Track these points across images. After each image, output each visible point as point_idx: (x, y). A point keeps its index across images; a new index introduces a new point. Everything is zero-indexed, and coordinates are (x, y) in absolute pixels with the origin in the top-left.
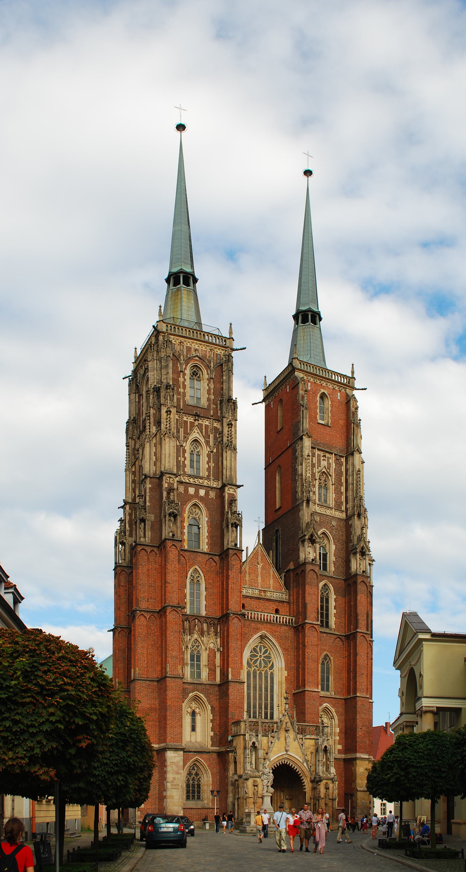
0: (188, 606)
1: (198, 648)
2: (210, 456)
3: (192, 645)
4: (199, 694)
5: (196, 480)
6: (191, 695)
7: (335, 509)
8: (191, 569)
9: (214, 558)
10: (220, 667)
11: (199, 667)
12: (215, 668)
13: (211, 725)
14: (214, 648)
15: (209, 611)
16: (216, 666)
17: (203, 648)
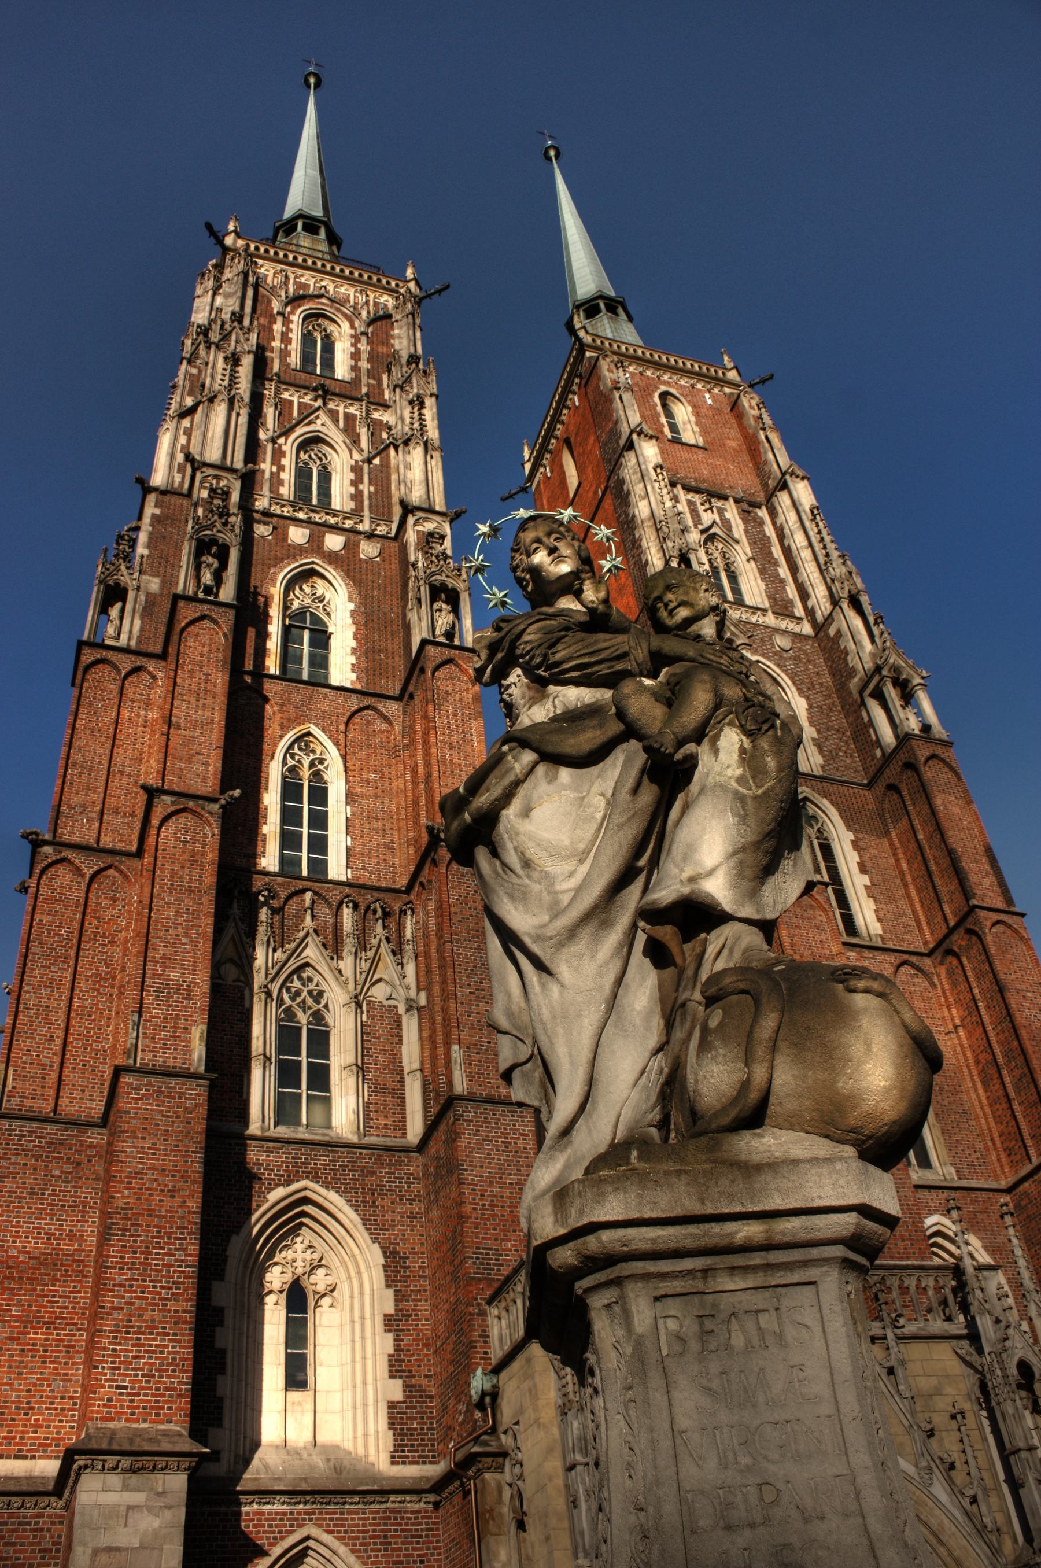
1: (318, 1002)
2: (361, 469)
4: (323, 1191)
5: (312, 515)
7: (774, 613)
8: (291, 733)
10: (421, 1070)
12: (402, 1081)
13: (386, 1343)
14: (391, 1002)
16: (406, 1070)
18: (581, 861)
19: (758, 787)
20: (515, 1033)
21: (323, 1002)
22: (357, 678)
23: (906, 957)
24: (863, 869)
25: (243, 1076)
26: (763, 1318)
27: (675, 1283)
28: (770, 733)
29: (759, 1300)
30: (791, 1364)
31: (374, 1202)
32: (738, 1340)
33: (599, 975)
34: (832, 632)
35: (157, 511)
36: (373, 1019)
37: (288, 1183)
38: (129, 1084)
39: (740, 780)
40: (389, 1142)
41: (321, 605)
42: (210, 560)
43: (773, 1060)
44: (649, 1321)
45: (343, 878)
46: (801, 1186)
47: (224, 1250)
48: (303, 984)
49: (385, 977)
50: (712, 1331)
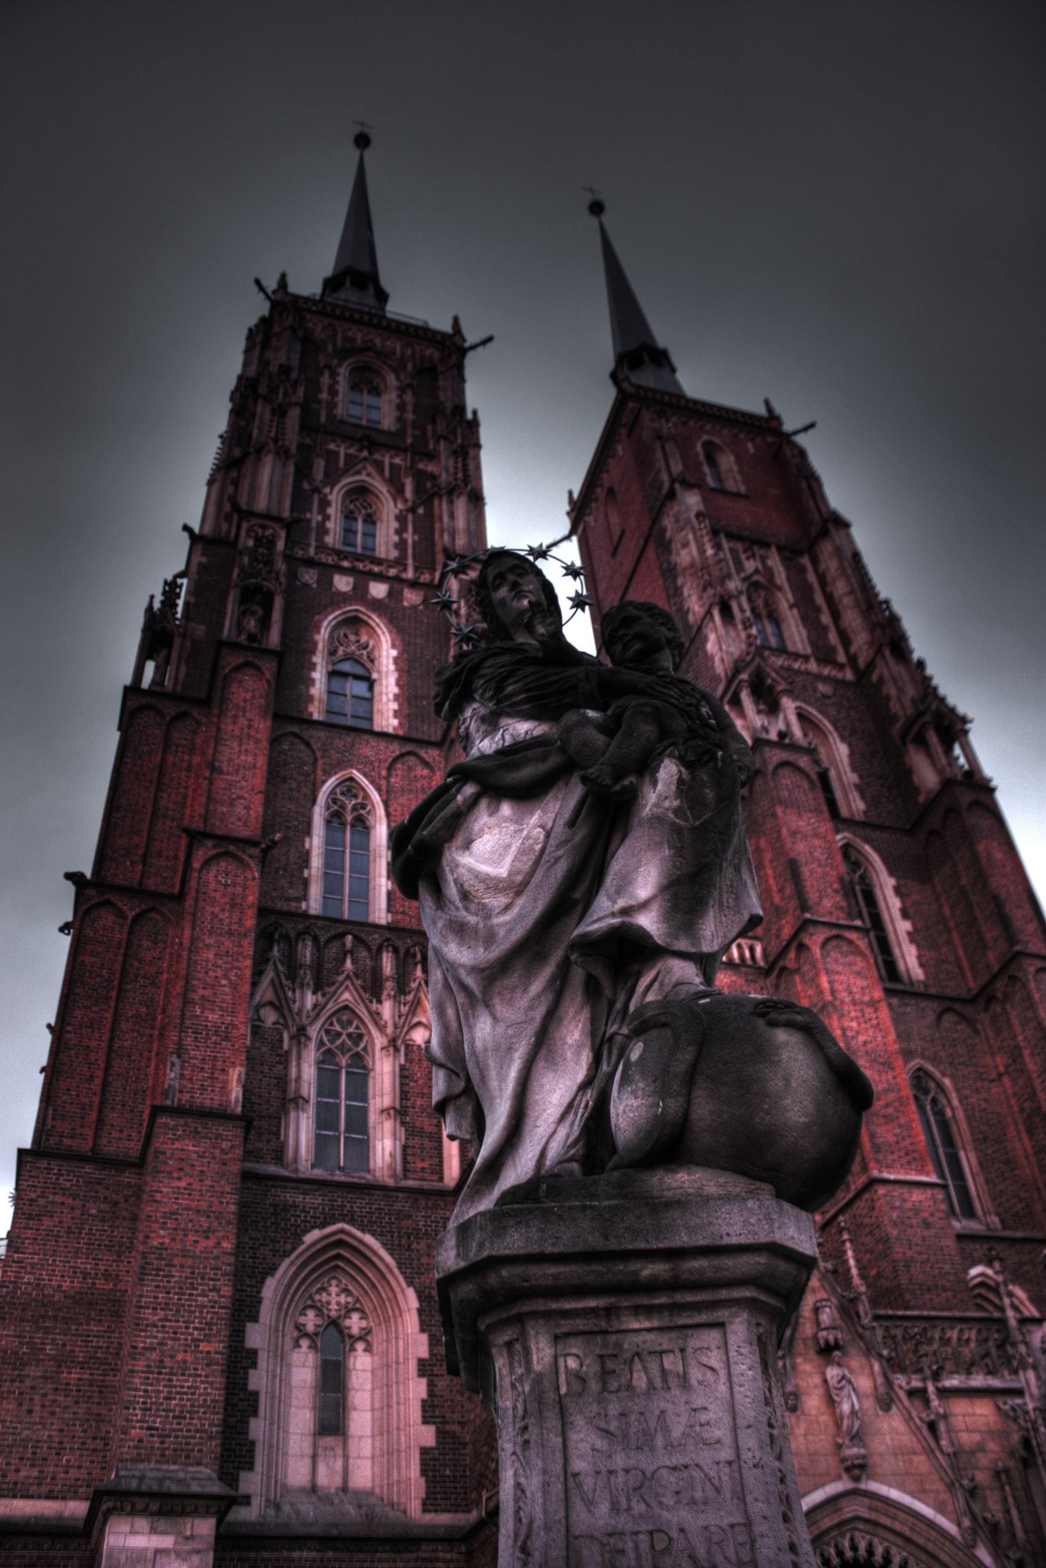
0: (315, 891)
3: (327, 1032)
4: (358, 1233)
6: (315, 1234)
9: (422, 752)
11: (359, 1122)
15: (403, 913)
17: (379, 1041)
18: (518, 894)
19: (695, 819)
20: (450, 1065)
21: (362, 1045)
22: (400, 724)
23: (949, 1004)
24: (905, 914)
25: (280, 1118)
26: (668, 1362)
27: (578, 1321)
28: (711, 764)
29: (665, 1341)
30: (694, 1406)
31: (409, 1246)
32: (640, 1381)
33: (531, 1008)
34: (874, 677)
35: (204, 560)
36: (411, 1063)
37: (323, 1225)
38: (166, 1125)
39: (677, 812)
40: (425, 1185)
41: (365, 652)
42: (255, 608)
43: (690, 1093)
44: (548, 1359)
45: (383, 922)
46: (711, 1223)
47: (259, 1292)
48: (342, 1027)
49: (424, 1020)
50: (614, 1371)
